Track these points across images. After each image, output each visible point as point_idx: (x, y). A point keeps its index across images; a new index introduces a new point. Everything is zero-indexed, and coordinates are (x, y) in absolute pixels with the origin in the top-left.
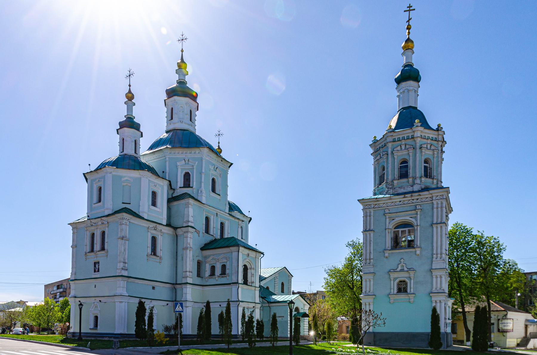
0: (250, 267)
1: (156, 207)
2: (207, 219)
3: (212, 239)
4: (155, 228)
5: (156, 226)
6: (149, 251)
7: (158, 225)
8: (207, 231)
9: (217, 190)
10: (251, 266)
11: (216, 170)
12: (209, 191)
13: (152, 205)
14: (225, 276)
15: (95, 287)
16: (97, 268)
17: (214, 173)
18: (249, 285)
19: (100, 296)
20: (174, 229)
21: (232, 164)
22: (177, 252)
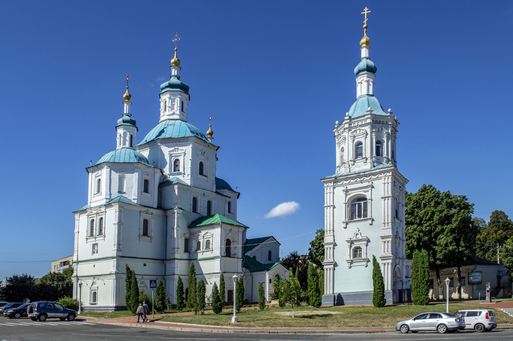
0: (233, 240)
1: (148, 193)
2: (195, 200)
3: (199, 217)
4: (147, 212)
5: (148, 210)
6: (142, 232)
7: (149, 209)
8: (195, 210)
9: (204, 174)
10: (234, 240)
11: (203, 155)
12: (197, 174)
13: (144, 192)
14: (209, 250)
15: (94, 266)
16: (96, 249)
17: (202, 157)
18: (231, 257)
19: (98, 274)
20: (164, 211)
21: (219, 147)
22: (166, 232)
